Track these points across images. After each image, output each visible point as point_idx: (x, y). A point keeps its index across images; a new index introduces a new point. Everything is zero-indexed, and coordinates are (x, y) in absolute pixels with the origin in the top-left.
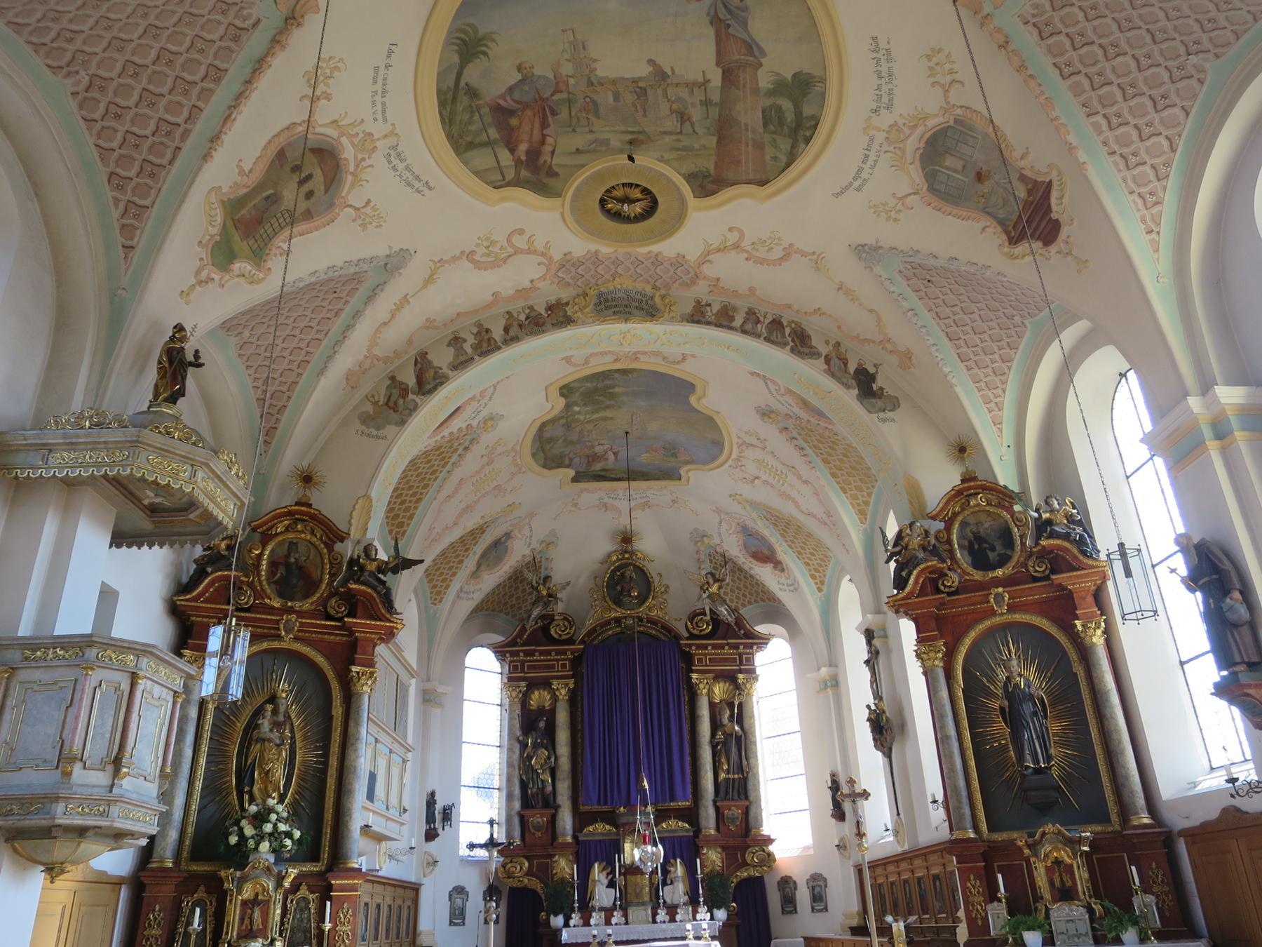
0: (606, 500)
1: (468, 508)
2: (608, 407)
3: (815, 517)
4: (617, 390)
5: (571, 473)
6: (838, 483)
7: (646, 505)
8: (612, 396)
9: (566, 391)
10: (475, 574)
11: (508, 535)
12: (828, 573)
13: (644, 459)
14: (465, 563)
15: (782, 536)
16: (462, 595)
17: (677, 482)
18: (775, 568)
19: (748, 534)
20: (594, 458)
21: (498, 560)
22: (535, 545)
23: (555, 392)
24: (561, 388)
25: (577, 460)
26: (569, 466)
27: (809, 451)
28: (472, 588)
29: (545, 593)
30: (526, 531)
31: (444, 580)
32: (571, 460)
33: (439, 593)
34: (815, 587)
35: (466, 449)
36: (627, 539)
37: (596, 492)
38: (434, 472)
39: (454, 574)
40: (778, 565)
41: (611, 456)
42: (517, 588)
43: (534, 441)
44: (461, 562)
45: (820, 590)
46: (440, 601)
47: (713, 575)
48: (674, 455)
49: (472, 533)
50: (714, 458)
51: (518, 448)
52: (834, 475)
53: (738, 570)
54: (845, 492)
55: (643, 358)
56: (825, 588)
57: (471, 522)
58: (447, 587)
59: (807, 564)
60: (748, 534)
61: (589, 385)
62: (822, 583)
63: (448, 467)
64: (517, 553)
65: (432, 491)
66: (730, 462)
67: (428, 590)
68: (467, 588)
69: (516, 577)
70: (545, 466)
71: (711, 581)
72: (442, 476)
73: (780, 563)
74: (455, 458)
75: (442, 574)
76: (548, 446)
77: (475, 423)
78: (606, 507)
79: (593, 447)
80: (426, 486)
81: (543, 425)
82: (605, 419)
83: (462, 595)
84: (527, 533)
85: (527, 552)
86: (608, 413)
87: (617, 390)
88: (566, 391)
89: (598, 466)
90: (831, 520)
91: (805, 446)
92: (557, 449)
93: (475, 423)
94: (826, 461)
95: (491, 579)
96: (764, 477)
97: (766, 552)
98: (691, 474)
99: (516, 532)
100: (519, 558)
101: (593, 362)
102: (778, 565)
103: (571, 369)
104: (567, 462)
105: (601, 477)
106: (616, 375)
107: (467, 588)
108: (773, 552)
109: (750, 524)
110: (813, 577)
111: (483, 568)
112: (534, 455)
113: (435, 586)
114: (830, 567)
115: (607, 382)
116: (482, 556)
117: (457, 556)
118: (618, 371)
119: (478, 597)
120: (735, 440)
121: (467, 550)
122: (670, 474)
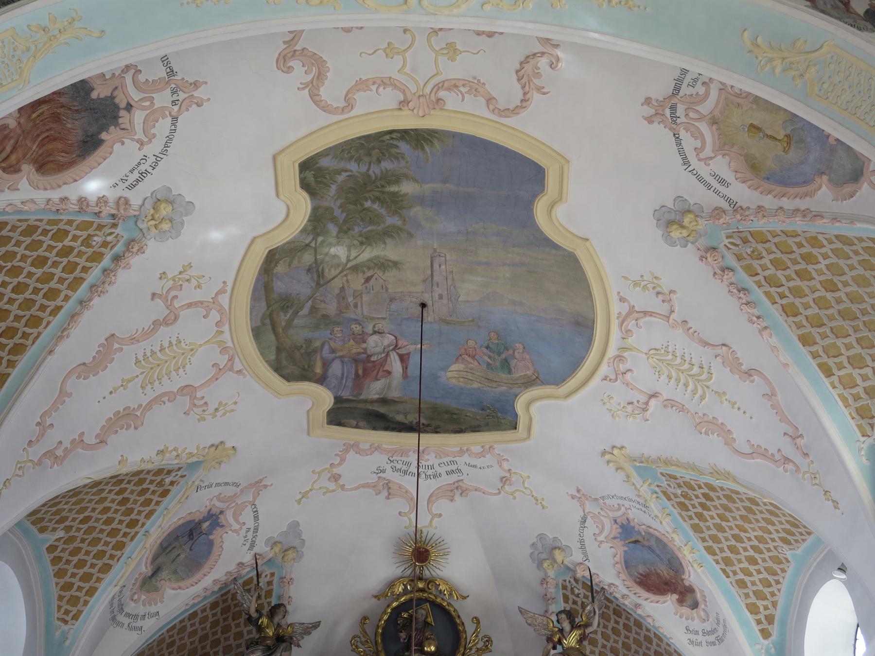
0: (389, 475)
1: (127, 419)
2: (388, 233)
3: (764, 454)
4: (407, 188)
5: (325, 398)
6: (815, 355)
7: (457, 489)
8: (396, 203)
9: (313, 174)
10: (149, 582)
11: (214, 519)
12: (781, 598)
13: (456, 375)
14: (128, 550)
15: (696, 529)
16: (121, 618)
17: (509, 435)
18: (681, 601)
19: (631, 537)
20: (367, 367)
21: (194, 566)
22: (261, 547)
23: (291, 177)
24: (305, 166)
25: (336, 368)
26: (321, 380)
27: (758, 294)
28: (141, 610)
29: (270, 632)
30: (247, 516)
31: (87, 577)
32: (326, 365)
33: (74, 601)
34: (756, 628)
35: (117, 258)
36: (421, 553)
37: (374, 452)
38: (52, 294)
39: (106, 568)
40: (686, 595)
41: (396, 367)
42: (226, 629)
43: (255, 297)
44: (120, 546)
45: (765, 634)
46: (76, 617)
47: (570, 615)
48: (506, 365)
49: (139, 477)
50: (575, 364)
51: (224, 300)
52: (806, 340)
53: (615, 612)
54: (828, 373)
55: (451, 100)
56: (775, 630)
57: (134, 452)
58: (91, 592)
59: (741, 584)
60: (631, 537)
61: (353, 166)
62: (770, 619)
63: (82, 291)
64: (230, 556)
65: (47, 334)
66: (604, 369)
67: (55, 592)
68: (131, 607)
69: (225, 604)
70: (278, 369)
71: (566, 626)
72: (68, 306)
73: (690, 590)
74: (95, 274)
75: (81, 564)
76: (283, 318)
77: (136, 198)
78: (389, 489)
79: (362, 338)
80: (35, 322)
81: (272, 258)
82: (383, 265)
83: (121, 618)
84: (250, 524)
85: (248, 559)
86: (389, 251)
87: (407, 188)
88: (313, 174)
89: (374, 389)
90: (799, 448)
91: (749, 282)
92: (300, 332)
93: (136, 198)
94: (789, 311)
95: (178, 599)
96: (667, 391)
97: (663, 570)
98: (533, 408)
99: (229, 516)
100: (232, 567)
101: (364, 103)
102: (686, 595)
103: (324, 119)
104: (318, 370)
105: (379, 418)
106: (404, 147)
107: (131, 607)
108: (676, 566)
109: (637, 516)
110: (753, 609)
111: (164, 574)
112: (257, 333)
113: (68, 586)
114: (784, 587)
115: (387, 165)
116: (166, 547)
117: (114, 533)
118: (405, 134)
119: (151, 628)
120: (616, 308)
121: (133, 524)
122: (497, 417)
